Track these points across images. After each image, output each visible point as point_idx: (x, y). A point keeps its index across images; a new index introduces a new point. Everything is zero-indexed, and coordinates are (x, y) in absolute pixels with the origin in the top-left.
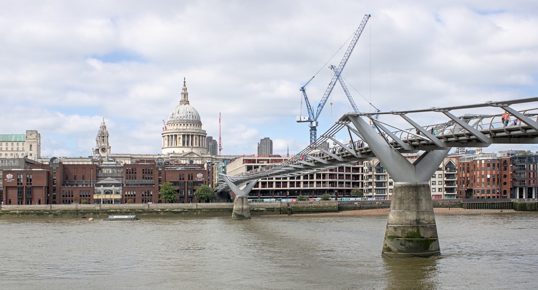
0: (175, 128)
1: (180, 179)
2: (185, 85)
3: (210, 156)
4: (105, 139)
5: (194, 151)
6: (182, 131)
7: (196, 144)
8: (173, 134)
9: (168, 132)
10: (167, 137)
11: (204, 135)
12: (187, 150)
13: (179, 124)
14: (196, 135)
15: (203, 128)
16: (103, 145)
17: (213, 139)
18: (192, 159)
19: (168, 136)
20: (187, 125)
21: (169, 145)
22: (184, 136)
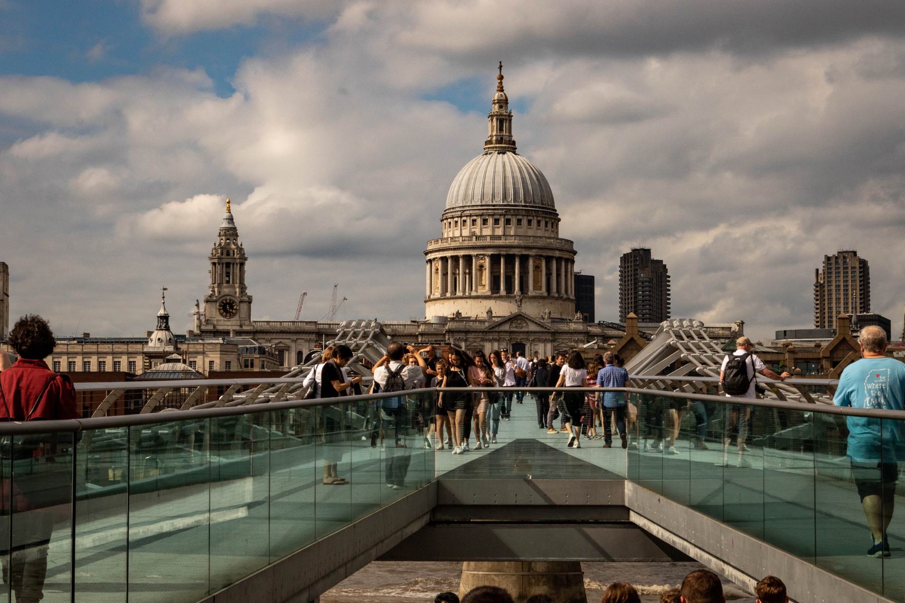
0: (466, 233)
3: (580, 327)
5: (531, 309)
6: (488, 242)
7: (537, 286)
9: (445, 245)
10: (439, 265)
11: (566, 255)
14: (538, 257)
16: (226, 291)
17: (655, 256)
18: (519, 338)
19: (444, 260)
21: (447, 291)
22: (495, 260)
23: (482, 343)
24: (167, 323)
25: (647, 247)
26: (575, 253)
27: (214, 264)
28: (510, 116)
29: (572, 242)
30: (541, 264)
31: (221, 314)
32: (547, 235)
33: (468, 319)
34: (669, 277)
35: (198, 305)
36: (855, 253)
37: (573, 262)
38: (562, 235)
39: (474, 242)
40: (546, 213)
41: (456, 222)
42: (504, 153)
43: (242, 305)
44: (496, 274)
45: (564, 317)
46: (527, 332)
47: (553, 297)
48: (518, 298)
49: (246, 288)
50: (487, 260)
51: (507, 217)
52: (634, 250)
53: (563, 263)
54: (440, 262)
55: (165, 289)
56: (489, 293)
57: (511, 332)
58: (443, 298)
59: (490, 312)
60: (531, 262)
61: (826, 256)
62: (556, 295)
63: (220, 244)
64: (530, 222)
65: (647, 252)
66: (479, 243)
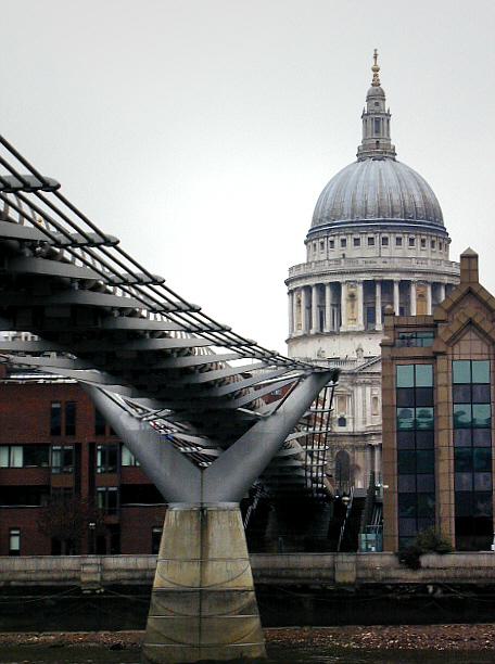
0: (336, 253)
1: (55, 431)
2: (376, 84)
6: (364, 267)
13: (350, 242)
19: (308, 289)
20: (385, 241)
21: (311, 327)
22: (369, 287)
23: (350, 387)
30: (426, 291)
32: (434, 257)
39: (344, 266)
41: (322, 243)
44: (370, 305)
50: (360, 288)
51: (383, 235)
54: (303, 293)
56: (362, 328)
58: (306, 337)
60: (413, 289)
64: (412, 240)
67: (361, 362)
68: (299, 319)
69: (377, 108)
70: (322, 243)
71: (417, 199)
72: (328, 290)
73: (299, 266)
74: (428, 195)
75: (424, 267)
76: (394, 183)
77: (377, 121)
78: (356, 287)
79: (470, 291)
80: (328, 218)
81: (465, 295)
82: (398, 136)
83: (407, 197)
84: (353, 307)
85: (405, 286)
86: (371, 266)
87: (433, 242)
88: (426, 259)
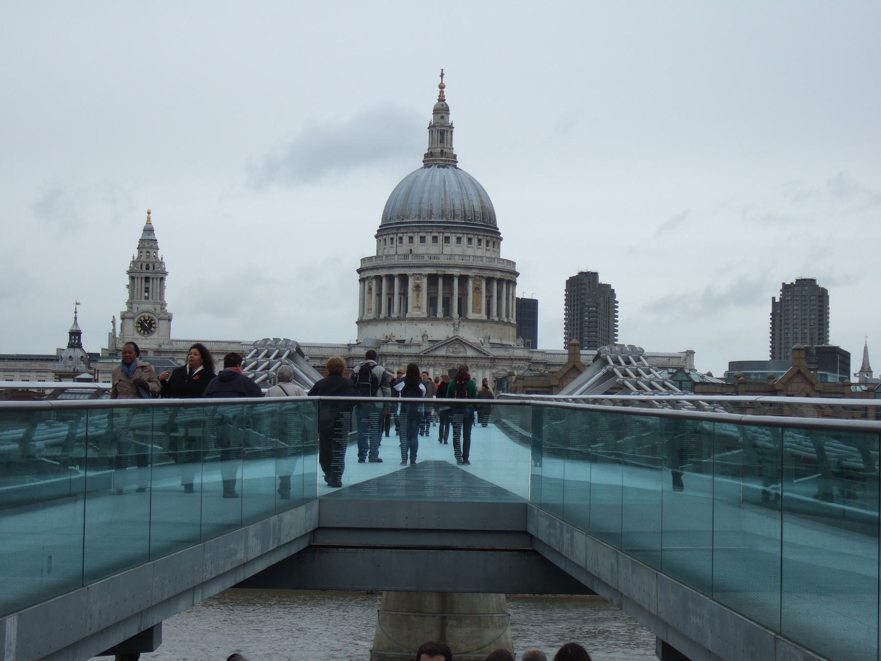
0: (401, 251)
2: (441, 99)
4: (154, 285)
5: (469, 334)
7: (477, 310)
8: (396, 272)
9: (380, 263)
11: (507, 277)
12: (440, 331)
13: (417, 239)
15: (506, 251)
17: (602, 280)
19: (379, 278)
20: (447, 239)
21: (380, 311)
22: (432, 279)
24: (79, 339)
25: (592, 269)
26: (517, 274)
27: (132, 278)
28: (451, 127)
29: (514, 263)
31: (139, 332)
32: (488, 255)
33: (401, 342)
34: (617, 302)
35: (114, 322)
36: (815, 280)
37: (515, 284)
38: (503, 256)
39: (411, 260)
40: (488, 231)
41: (392, 239)
42: (444, 167)
43: (161, 322)
44: (433, 295)
45: (504, 342)
46: (465, 358)
47: (493, 322)
48: (457, 322)
49: (166, 305)
50: (425, 280)
51: (446, 235)
52: (581, 274)
53: (505, 285)
54: (374, 282)
55: (77, 304)
56: (425, 315)
57: (447, 357)
58: (376, 320)
59: (424, 336)
60: (471, 283)
61: (784, 284)
62: (496, 319)
63: (140, 257)
64: (470, 240)
65: (595, 275)
66: (415, 261)
67: (426, 346)
68: (370, 303)
69: (442, 121)
70: (392, 239)
71: (476, 204)
72: (397, 281)
73: (371, 258)
74: (484, 199)
75: (480, 264)
76: (455, 188)
77: (442, 133)
78: (421, 280)
79: (574, 367)
80: (398, 217)
81: (570, 370)
82: (460, 144)
83: (466, 203)
84: (418, 296)
85: (463, 279)
86: (435, 261)
87: (488, 242)
88: (481, 257)
